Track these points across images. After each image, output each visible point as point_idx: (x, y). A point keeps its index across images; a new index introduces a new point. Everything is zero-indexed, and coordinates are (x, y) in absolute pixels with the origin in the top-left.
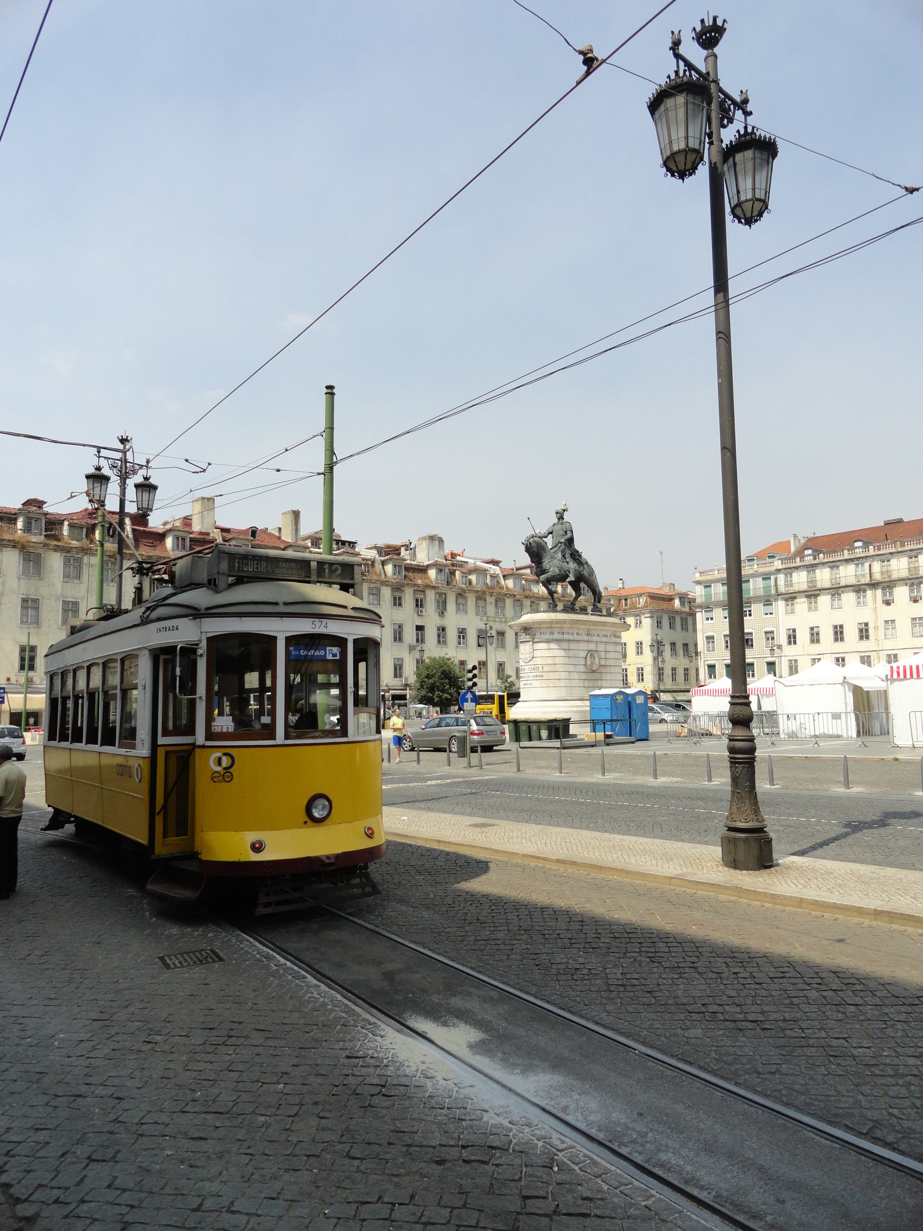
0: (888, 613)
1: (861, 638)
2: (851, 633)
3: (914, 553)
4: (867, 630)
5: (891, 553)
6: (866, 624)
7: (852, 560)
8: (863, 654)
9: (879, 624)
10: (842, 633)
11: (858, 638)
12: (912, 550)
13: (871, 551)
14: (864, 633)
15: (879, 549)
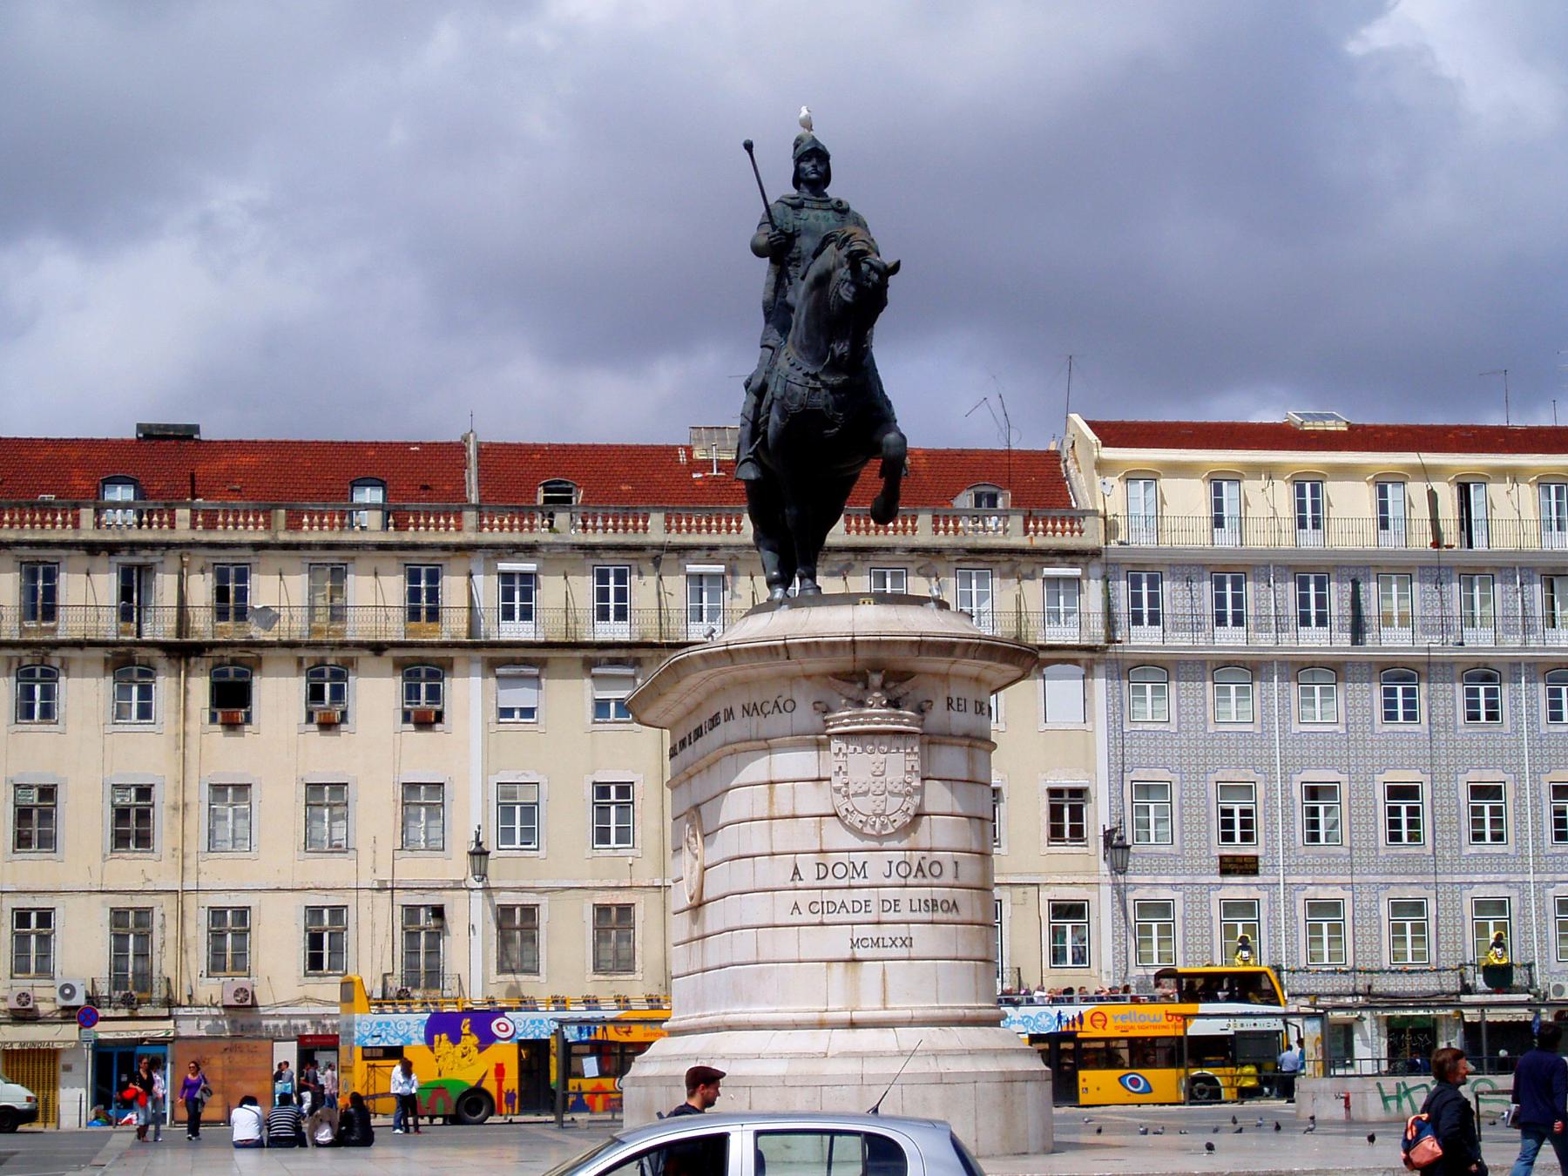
0: (224, 755)
1: (120, 840)
2: (84, 819)
3: (333, 557)
4: (144, 816)
5: (258, 546)
6: (144, 792)
7: (112, 548)
8: (123, 902)
9: (192, 796)
10: (47, 816)
11: (109, 840)
12: (330, 546)
13: (183, 526)
14: (132, 823)
15: (210, 525)
